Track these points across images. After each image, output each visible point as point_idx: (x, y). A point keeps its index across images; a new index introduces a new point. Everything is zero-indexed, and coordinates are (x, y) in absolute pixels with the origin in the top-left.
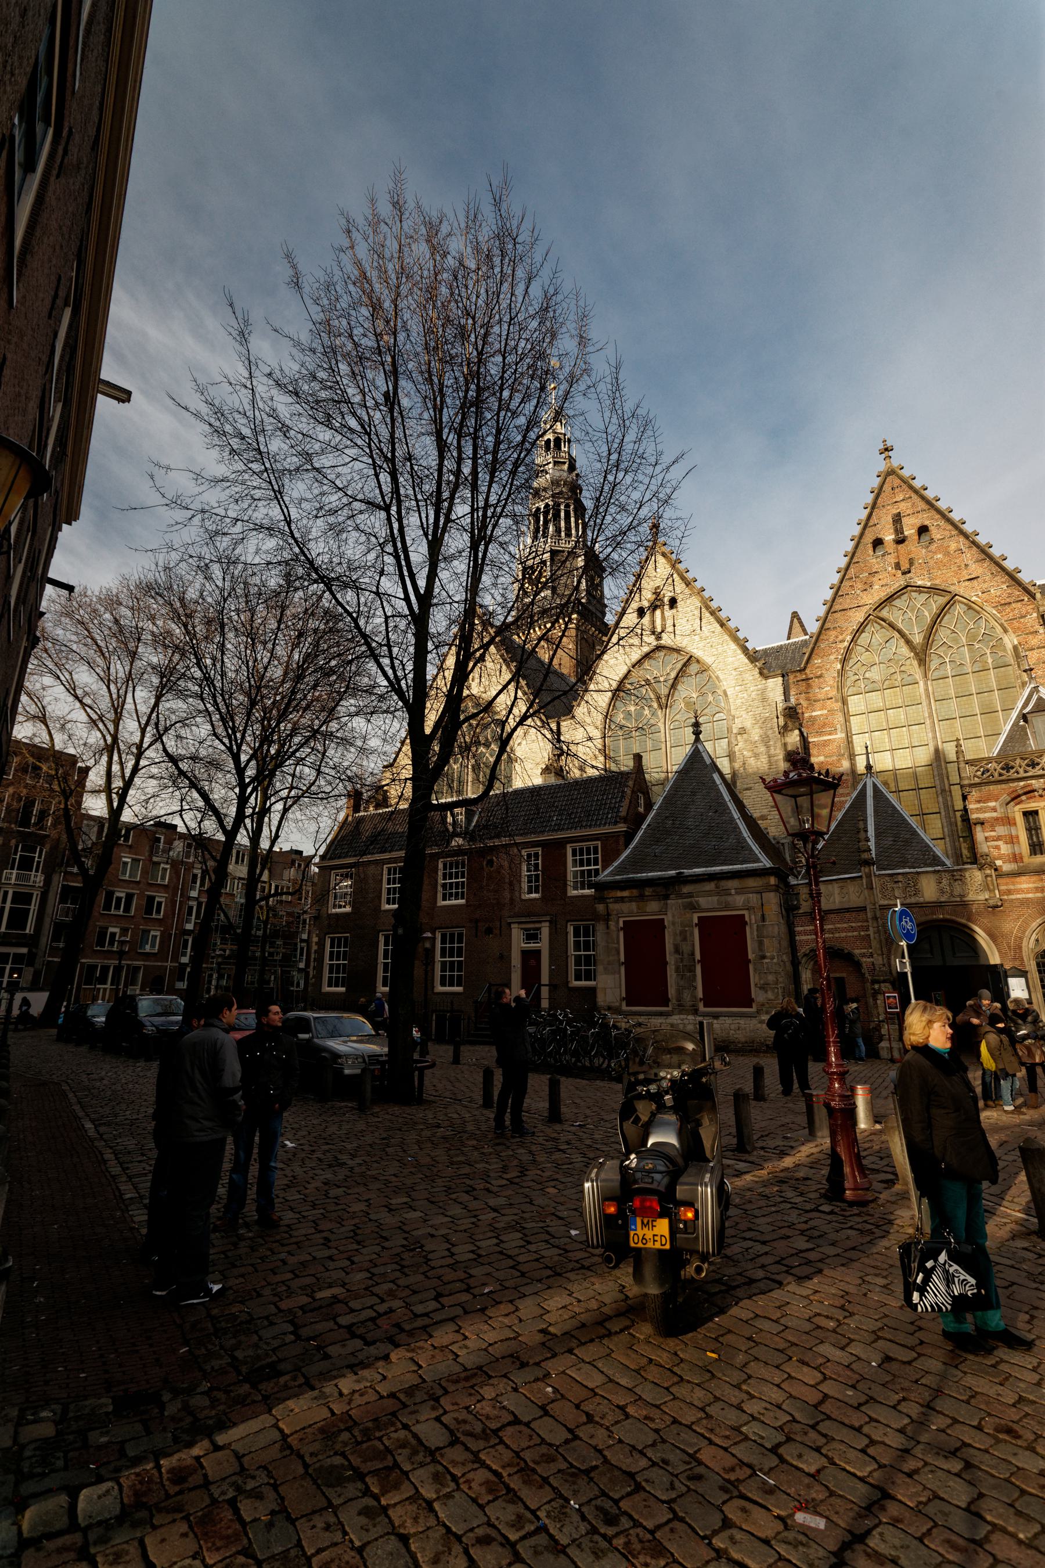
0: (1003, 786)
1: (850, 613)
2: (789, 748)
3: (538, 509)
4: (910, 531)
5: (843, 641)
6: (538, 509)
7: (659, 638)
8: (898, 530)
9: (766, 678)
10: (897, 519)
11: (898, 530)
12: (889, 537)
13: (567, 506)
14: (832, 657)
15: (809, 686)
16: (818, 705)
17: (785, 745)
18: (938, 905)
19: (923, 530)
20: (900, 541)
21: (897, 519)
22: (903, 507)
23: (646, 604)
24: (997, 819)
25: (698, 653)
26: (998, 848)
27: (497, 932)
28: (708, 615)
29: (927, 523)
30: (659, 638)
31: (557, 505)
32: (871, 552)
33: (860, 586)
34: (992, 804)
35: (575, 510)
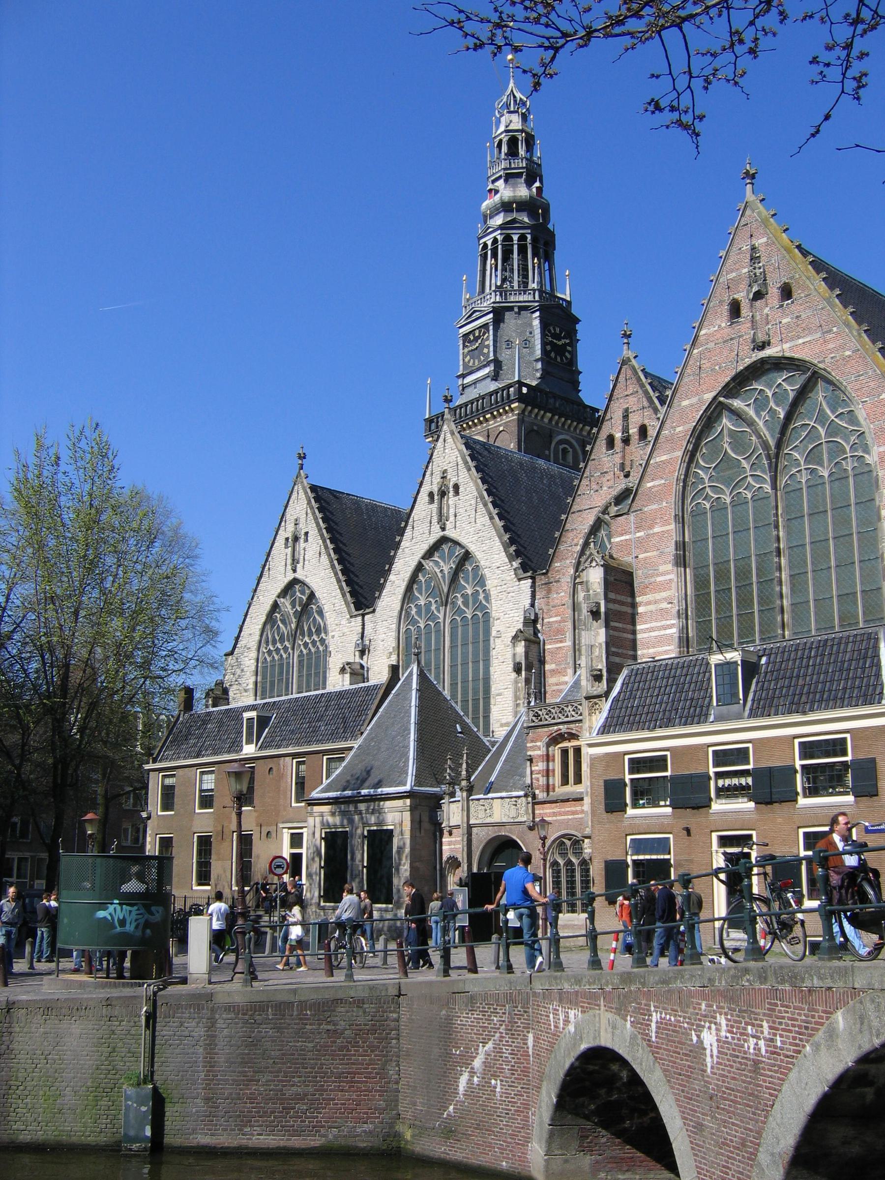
0: (546, 729)
1: (584, 514)
2: (518, 660)
3: (485, 246)
4: (633, 431)
5: (576, 545)
6: (485, 246)
7: (443, 529)
8: (625, 430)
9: (520, 580)
10: (626, 417)
11: (625, 430)
12: (618, 435)
13: (522, 238)
14: (568, 561)
15: (549, 591)
16: (554, 611)
17: (514, 655)
18: (502, 825)
19: (643, 431)
20: (626, 441)
21: (626, 417)
22: (632, 403)
23: (435, 490)
24: (540, 756)
25: (472, 548)
26: (538, 780)
27: (274, 835)
28: (481, 506)
29: (646, 422)
30: (443, 529)
31: (508, 238)
32: (604, 449)
33: (594, 486)
34: (538, 744)
35: (534, 240)
